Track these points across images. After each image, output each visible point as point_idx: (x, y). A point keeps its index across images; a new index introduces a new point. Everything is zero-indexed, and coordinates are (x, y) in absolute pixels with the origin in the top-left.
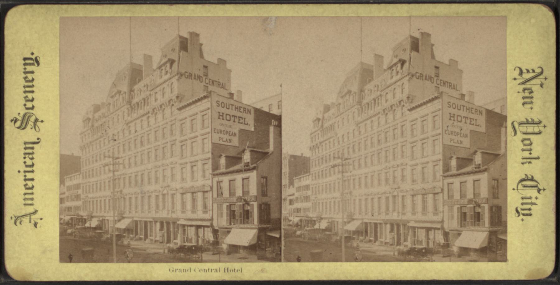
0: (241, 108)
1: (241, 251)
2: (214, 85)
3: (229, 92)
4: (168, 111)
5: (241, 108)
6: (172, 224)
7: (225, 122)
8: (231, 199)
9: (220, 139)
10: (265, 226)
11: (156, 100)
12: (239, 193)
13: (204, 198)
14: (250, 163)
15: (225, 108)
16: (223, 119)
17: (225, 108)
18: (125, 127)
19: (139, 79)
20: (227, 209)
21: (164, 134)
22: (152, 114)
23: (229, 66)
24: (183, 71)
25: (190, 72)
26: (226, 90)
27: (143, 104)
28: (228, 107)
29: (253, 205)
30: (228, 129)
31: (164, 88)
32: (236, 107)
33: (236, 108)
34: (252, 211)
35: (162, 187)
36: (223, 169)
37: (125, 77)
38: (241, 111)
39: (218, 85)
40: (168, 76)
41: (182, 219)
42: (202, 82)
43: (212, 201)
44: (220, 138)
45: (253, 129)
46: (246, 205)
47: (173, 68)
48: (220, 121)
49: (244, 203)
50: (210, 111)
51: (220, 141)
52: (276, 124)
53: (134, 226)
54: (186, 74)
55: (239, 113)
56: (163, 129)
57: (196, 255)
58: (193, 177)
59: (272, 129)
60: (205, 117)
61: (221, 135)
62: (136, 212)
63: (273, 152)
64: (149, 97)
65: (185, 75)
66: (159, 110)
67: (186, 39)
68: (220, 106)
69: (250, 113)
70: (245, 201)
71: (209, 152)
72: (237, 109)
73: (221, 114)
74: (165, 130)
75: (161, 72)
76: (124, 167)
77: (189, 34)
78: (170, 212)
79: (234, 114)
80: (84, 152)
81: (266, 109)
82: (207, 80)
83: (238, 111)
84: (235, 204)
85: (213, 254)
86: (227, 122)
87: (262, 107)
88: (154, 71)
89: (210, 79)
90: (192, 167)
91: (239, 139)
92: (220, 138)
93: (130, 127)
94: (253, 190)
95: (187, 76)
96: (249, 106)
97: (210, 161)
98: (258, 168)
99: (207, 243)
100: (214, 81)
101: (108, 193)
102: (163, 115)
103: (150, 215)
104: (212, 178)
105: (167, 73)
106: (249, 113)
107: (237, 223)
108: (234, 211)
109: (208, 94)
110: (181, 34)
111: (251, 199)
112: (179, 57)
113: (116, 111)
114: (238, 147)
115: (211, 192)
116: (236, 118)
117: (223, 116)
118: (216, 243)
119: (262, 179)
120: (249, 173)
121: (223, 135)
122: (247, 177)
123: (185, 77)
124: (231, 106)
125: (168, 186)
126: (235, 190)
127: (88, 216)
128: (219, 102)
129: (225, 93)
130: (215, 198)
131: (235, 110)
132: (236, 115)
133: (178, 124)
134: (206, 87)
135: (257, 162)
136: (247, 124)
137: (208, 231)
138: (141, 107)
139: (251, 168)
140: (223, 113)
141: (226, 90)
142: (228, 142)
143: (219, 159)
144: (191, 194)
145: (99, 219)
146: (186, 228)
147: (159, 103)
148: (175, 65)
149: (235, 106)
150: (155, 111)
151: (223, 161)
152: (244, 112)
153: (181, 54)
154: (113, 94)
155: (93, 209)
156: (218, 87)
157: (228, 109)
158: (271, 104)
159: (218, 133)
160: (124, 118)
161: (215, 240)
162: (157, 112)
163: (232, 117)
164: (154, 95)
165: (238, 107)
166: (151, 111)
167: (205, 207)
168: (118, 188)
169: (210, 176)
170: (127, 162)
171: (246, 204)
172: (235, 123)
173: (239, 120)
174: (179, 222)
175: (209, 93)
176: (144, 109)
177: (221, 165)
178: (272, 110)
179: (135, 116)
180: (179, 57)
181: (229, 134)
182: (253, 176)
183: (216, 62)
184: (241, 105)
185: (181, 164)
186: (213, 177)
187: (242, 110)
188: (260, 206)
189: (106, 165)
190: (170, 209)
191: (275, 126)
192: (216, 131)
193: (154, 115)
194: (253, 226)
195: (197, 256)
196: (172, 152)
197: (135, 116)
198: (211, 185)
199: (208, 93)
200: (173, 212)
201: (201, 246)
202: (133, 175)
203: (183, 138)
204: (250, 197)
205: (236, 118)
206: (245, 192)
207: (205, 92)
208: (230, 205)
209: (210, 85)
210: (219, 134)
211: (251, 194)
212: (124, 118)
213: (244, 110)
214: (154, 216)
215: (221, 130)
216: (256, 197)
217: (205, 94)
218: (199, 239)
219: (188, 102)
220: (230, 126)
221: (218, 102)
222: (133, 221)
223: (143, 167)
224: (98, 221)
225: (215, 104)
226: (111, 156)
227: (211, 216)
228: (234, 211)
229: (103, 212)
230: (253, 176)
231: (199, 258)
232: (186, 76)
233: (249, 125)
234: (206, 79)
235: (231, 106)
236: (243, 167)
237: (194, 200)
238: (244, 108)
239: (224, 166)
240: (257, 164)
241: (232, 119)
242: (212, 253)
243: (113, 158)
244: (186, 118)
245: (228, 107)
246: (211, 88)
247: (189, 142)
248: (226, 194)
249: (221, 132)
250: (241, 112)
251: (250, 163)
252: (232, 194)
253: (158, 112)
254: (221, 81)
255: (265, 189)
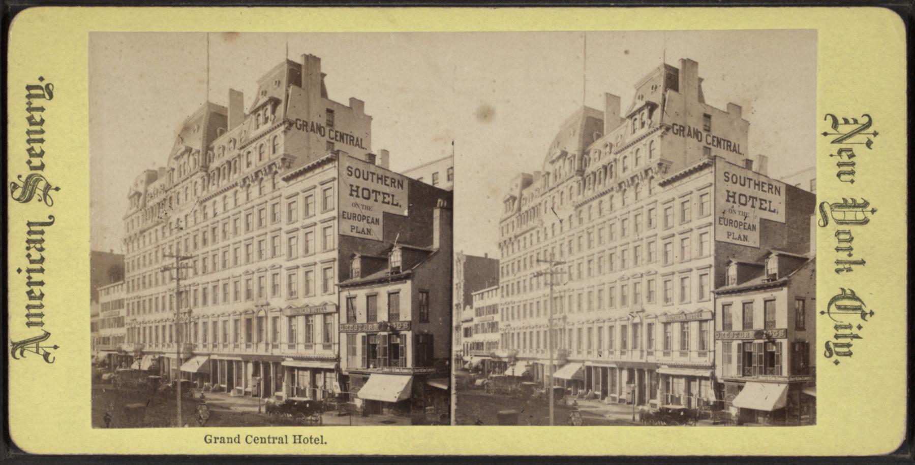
0: (387, 179)
1: (385, 410)
2: (343, 142)
3: (368, 152)
4: (267, 185)
5: (387, 179)
6: (273, 366)
7: (360, 201)
8: (370, 325)
9: (352, 229)
10: (425, 370)
11: (249, 164)
12: (383, 316)
13: (326, 325)
14: (401, 268)
15: (361, 178)
16: (357, 196)
17: (361, 178)
18: (197, 207)
19: (221, 130)
20: (363, 343)
21: (260, 220)
22: (241, 187)
23: (368, 111)
24: (293, 118)
25: (306, 120)
26: (363, 148)
27: (226, 171)
28: (365, 177)
29: (405, 335)
30: (366, 213)
31: (262, 146)
32: (380, 176)
33: (378, 178)
34: (403, 346)
35: (257, 306)
36: (356, 277)
37: (198, 128)
38: (387, 183)
39: (350, 140)
40: (269, 125)
41: (290, 357)
42: (324, 136)
43: (339, 330)
44: (352, 226)
45: (406, 213)
46: (395, 336)
47: (277, 114)
48: (353, 199)
49: (391, 333)
50: (336, 182)
51: (352, 231)
52: (443, 205)
53: (211, 370)
54: (299, 122)
55: (383, 186)
56: (260, 211)
57: (312, 416)
58: (307, 291)
59: (437, 213)
60: (329, 193)
61: (355, 223)
62: (236, 346)
63: (438, 251)
64: (237, 159)
65: (296, 124)
66: (253, 181)
67: (299, 66)
68: (354, 174)
69: (402, 186)
70: (392, 329)
71: (334, 250)
72: (380, 181)
73: (354, 188)
74: (263, 212)
75: (257, 120)
76: (196, 273)
77: (303, 57)
78: (270, 347)
79: (375, 189)
80: (130, 247)
81: (428, 181)
82: (331, 132)
83: (382, 184)
84: (376, 335)
85: (339, 415)
86: (365, 202)
87: (422, 178)
88: (246, 116)
89: (337, 132)
90: (307, 273)
91: (383, 229)
92: (353, 228)
93: (205, 207)
94: (406, 312)
95: (300, 125)
96: (401, 175)
97: (336, 263)
98: (414, 276)
99: (329, 397)
100: (343, 134)
101: (170, 315)
102: (260, 189)
103: (237, 351)
104: (339, 292)
105: (266, 120)
106: (400, 188)
107: (380, 366)
108: (375, 346)
109: (334, 155)
110: (290, 59)
111: (402, 327)
112: (287, 96)
113: (183, 181)
114: (382, 242)
115: (336, 315)
116: (379, 194)
117: (357, 191)
118: (345, 398)
119: (421, 294)
120: (400, 283)
121: (357, 222)
122: (397, 291)
123: (296, 127)
124: (370, 176)
125: (268, 304)
126: (375, 311)
127: (135, 351)
128: (352, 168)
129: (360, 154)
130: (344, 325)
131: (378, 182)
132: (378, 190)
133: (284, 202)
134: (330, 145)
135: (413, 266)
136: (397, 205)
137: (331, 378)
138: (224, 174)
139: (402, 277)
140: (358, 187)
141: (363, 148)
142: (365, 234)
143: (351, 261)
144: (322, 316)
145: (154, 356)
146: (296, 371)
147: (253, 168)
148: (280, 109)
149: (378, 175)
150: (248, 182)
151: (356, 265)
152: (391, 186)
153: (290, 91)
154: (179, 153)
155: (144, 341)
156: (350, 144)
157: (367, 179)
158: (437, 173)
159: (350, 219)
160: (195, 194)
161: (343, 392)
162: (250, 183)
163: (373, 193)
164: (245, 157)
165: (382, 176)
166: (240, 181)
167: (327, 338)
168: (186, 307)
169: (336, 288)
170: (200, 264)
171: (393, 334)
172: (376, 203)
173: (384, 198)
174: (284, 363)
175: (336, 154)
176: (229, 179)
177: (354, 271)
178: (438, 183)
179: (213, 189)
180: (287, 96)
181: (368, 220)
182: (406, 289)
183: (347, 104)
184: (388, 174)
185: (289, 269)
186: (340, 290)
187: (389, 182)
188: (416, 339)
189: (166, 269)
190: (270, 341)
191: (442, 208)
192: (346, 216)
193: (244, 188)
194: (406, 371)
195: (313, 418)
196: (274, 248)
197: (213, 189)
198: (337, 303)
199: (334, 153)
200: (275, 347)
201: (321, 402)
202: (210, 287)
203: (291, 227)
204: (400, 323)
205: (379, 194)
206: (394, 316)
207: (329, 152)
208: (368, 336)
209: (336, 140)
210: (351, 220)
211: (402, 318)
212: (195, 194)
213: (392, 182)
214: (244, 353)
215: (354, 214)
216: (410, 323)
217: (329, 155)
218: (317, 390)
219: (301, 168)
220: (369, 208)
221: (350, 169)
222: (209, 361)
223: (226, 273)
224: (152, 360)
225: (345, 172)
226: (175, 254)
227: (336, 353)
228: (375, 346)
229: (161, 346)
230: (406, 289)
231: (316, 421)
232: (299, 126)
233: (400, 206)
234: (330, 131)
235: (370, 176)
236: (390, 274)
237: (309, 327)
238: (392, 179)
239: (358, 272)
240: (412, 270)
241: (373, 195)
242: (338, 413)
243: (177, 258)
244: (297, 194)
245: (365, 177)
246: (338, 146)
247: (301, 234)
248: (362, 318)
249: (354, 216)
250: (388, 185)
251: (401, 268)
252: (371, 316)
253: (252, 184)
254: (356, 134)
255: (426, 312)
